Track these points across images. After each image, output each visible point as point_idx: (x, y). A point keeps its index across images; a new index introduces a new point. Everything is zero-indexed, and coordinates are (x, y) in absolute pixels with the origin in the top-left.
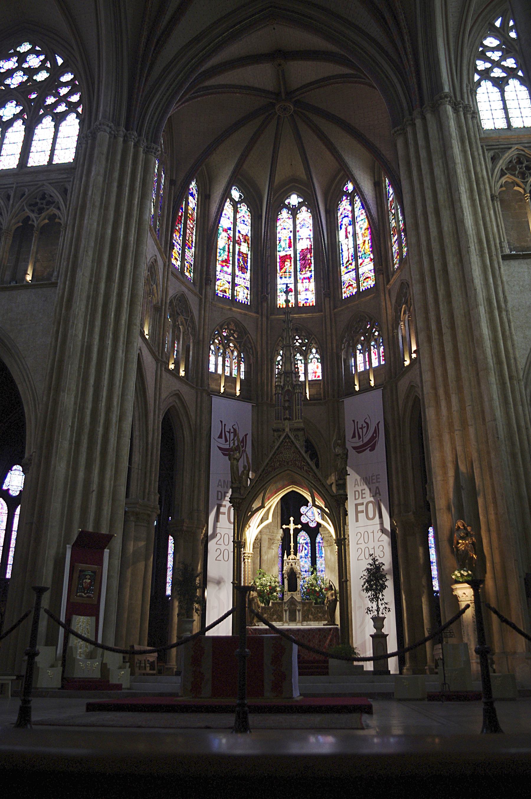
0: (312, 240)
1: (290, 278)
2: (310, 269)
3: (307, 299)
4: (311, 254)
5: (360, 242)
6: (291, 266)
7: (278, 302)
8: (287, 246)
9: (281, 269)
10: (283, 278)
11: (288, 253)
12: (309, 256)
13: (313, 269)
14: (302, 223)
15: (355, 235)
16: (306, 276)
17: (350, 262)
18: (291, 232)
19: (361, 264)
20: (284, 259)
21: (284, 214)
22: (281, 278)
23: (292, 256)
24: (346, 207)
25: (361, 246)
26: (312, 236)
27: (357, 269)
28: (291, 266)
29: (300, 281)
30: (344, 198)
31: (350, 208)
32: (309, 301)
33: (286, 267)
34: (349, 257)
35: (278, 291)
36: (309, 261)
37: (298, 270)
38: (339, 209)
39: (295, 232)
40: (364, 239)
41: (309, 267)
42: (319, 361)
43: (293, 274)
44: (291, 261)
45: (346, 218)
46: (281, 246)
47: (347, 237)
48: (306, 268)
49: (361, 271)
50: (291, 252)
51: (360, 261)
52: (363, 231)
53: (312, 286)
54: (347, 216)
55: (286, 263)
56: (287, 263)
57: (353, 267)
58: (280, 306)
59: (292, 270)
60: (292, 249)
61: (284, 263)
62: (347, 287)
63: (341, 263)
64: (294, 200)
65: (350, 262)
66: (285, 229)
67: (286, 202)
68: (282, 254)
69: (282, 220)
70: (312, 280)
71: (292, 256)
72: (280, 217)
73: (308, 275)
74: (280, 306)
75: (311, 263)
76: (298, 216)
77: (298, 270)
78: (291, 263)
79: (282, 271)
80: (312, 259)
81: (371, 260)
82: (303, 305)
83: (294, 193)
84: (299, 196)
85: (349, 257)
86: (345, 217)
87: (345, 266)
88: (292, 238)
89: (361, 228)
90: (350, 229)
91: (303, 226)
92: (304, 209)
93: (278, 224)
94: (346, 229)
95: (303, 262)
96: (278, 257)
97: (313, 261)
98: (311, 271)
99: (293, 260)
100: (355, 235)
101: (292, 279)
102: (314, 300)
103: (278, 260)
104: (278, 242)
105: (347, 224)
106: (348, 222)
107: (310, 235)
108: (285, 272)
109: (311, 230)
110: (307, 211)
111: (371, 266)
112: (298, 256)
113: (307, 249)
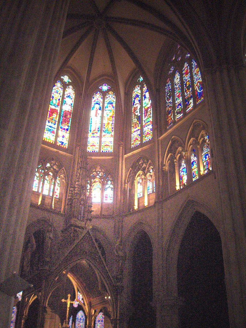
0: (72, 107)
1: (54, 124)
2: (68, 125)
3: (63, 143)
4: (70, 116)
5: (105, 121)
6: (56, 117)
7: (44, 136)
8: (57, 104)
9: (50, 116)
10: (50, 123)
11: (56, 108)
12: (69, 116)
13: (70, 125)
14: (68, 95)
15: (102, 117)
16: (64, 127)
17: (96, 131)
18: (61, 96)
19: (104, 136)
20: (53, 111)
21: (58, 85)
22: (49, 122)
23: (59, 111)
24: (99, 98)
25: (106, 125)
26: (73, 105)
27: (101, 137)
28: (56, 117)
29: (60, 129)
30: (98, 93)
31: (102, 100)
32: (63, 144)
33: (53, 116)
34: (96, 128)
35: (46, 129)
36: (68, 120)
37: (61, 122)
38: (94, 98)
39: (63, 98)
40: (109, 122)
41: (68, 124)
42: (59, 185)
43: (57, 123)
44: (57, 114)
45: (98, 105)
46: (53, 102)
47: (96, 116)
48: (66, 123)
49: (103, 139)
50: (58, 109)
51: (103, 134)
52: (109, 117)
53: (67, 135)
54: (99, 104)
55: (54, 114)
56: (54, 115)
57: (98, 134)
58: (44, 139)
59: (57, 120)
60: (59, 107)
61: (53, 114)
62: (91, 146)
63: (90, 129)
64: (66, 79)
65: (96, 131)
66: (57, 93)
67: (62, 77)
68: (53, 107)
69: (56, 87)
70: (68, 132)
71: (59, 111)
72: (56, 84)
73: (67, 128)
74: (44, 139)
75: (69, 121)
76: (67, 89)
77: (61, 122)
78: (57, 115)
79: (50, 118)
80: (71, 119)
81: (112, 136)
82: (60, 145)
83: (67, 75)
84: (70, 78)
85: (96, 128)
86: (97, 103)
87: (92, 132)
88: (61, 100)
89: (108, 115)
90: (100, 112)
91: (68, 96)
92: (71, 87)
93: (54, 88)
94: (97, 111)
95: (65, 118)
96: (50, 108)
97: (70, 121)
98: (68, 126)
99: (59, 114)
100: (102, 117)
101: (56, 125)
102: (67, 145)
103: (49, 110)
104: (51, 99)
105: (98, 109)
106: (99, 107)
107: (71, 104)
108: (52, 119)
109: (73, 102)
110: (73, 89)
111: (112, 139)
112: (62, 113)
113: (68, 111)
